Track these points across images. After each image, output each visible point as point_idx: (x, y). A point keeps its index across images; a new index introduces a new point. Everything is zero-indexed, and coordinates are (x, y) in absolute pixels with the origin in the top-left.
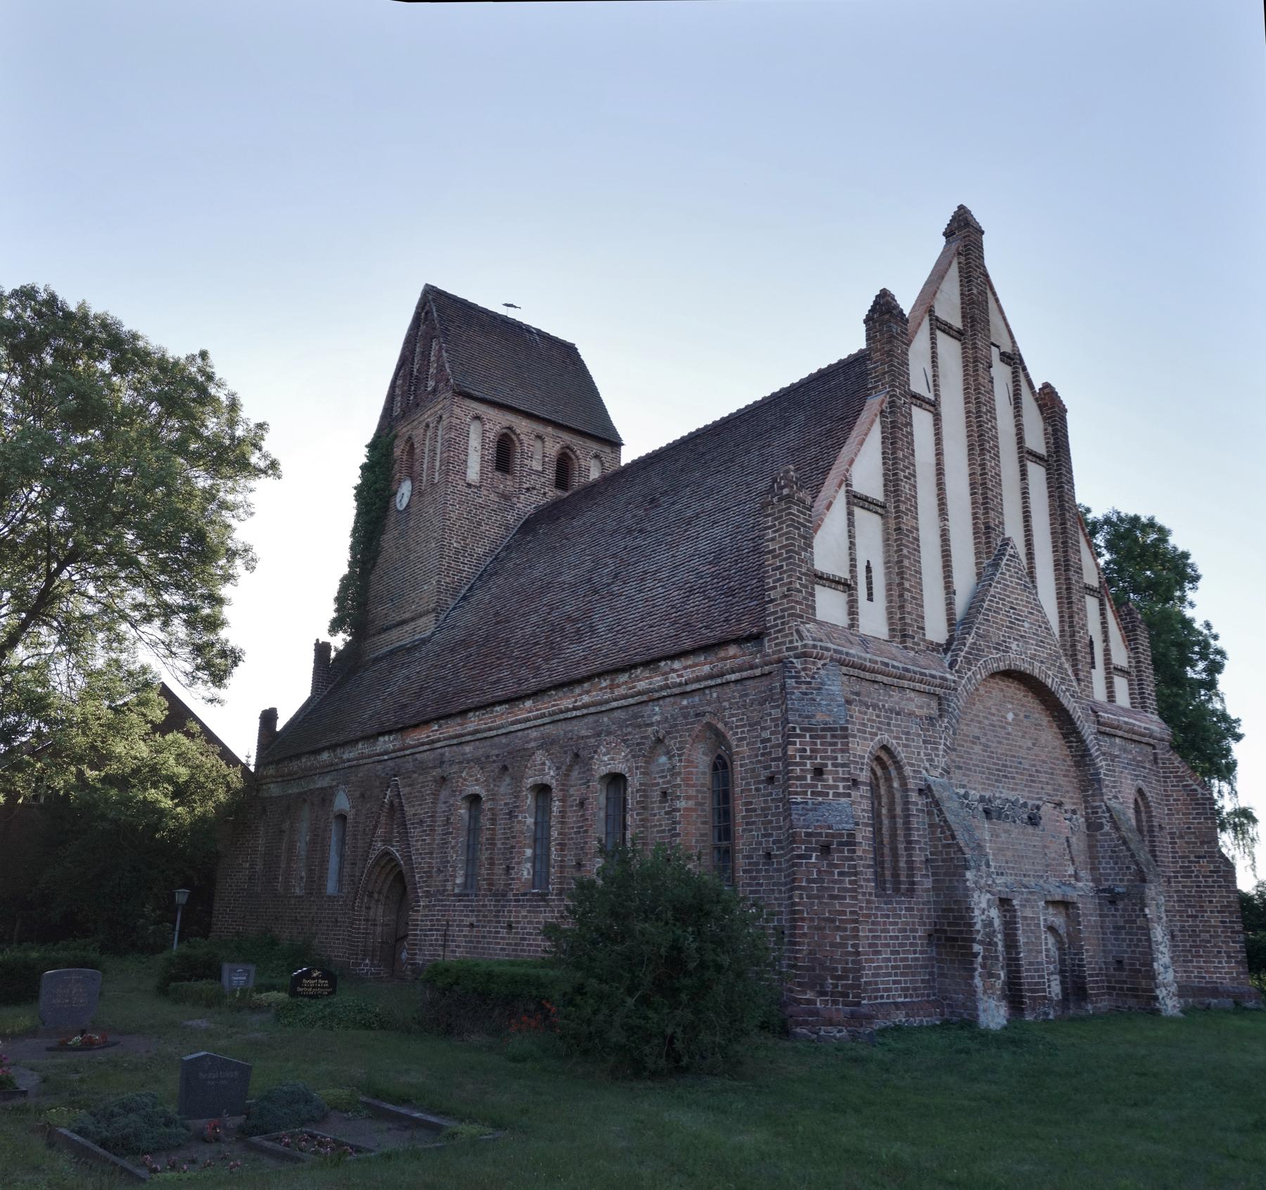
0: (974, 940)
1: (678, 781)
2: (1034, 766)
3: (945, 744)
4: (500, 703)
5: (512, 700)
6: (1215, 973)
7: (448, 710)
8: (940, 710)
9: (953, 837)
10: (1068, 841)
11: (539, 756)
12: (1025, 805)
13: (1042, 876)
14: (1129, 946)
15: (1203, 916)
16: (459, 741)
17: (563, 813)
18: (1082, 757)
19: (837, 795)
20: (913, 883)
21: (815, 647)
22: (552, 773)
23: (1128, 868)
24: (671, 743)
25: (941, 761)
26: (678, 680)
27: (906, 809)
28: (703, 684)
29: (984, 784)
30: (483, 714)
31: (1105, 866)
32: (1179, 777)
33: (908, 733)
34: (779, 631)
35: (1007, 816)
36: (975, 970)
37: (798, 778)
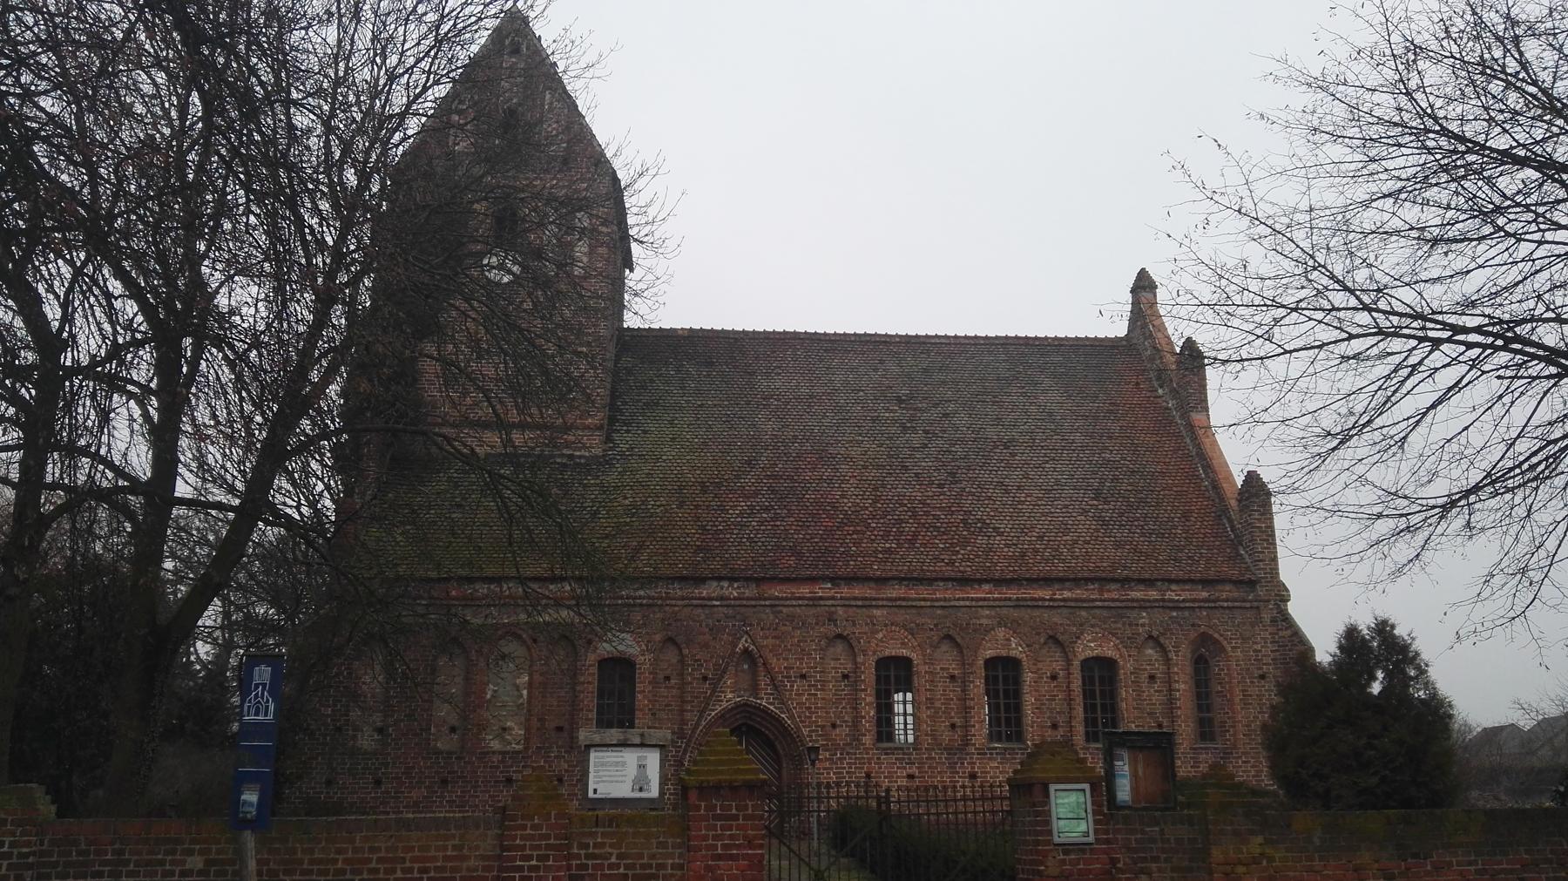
16: (868, 603)
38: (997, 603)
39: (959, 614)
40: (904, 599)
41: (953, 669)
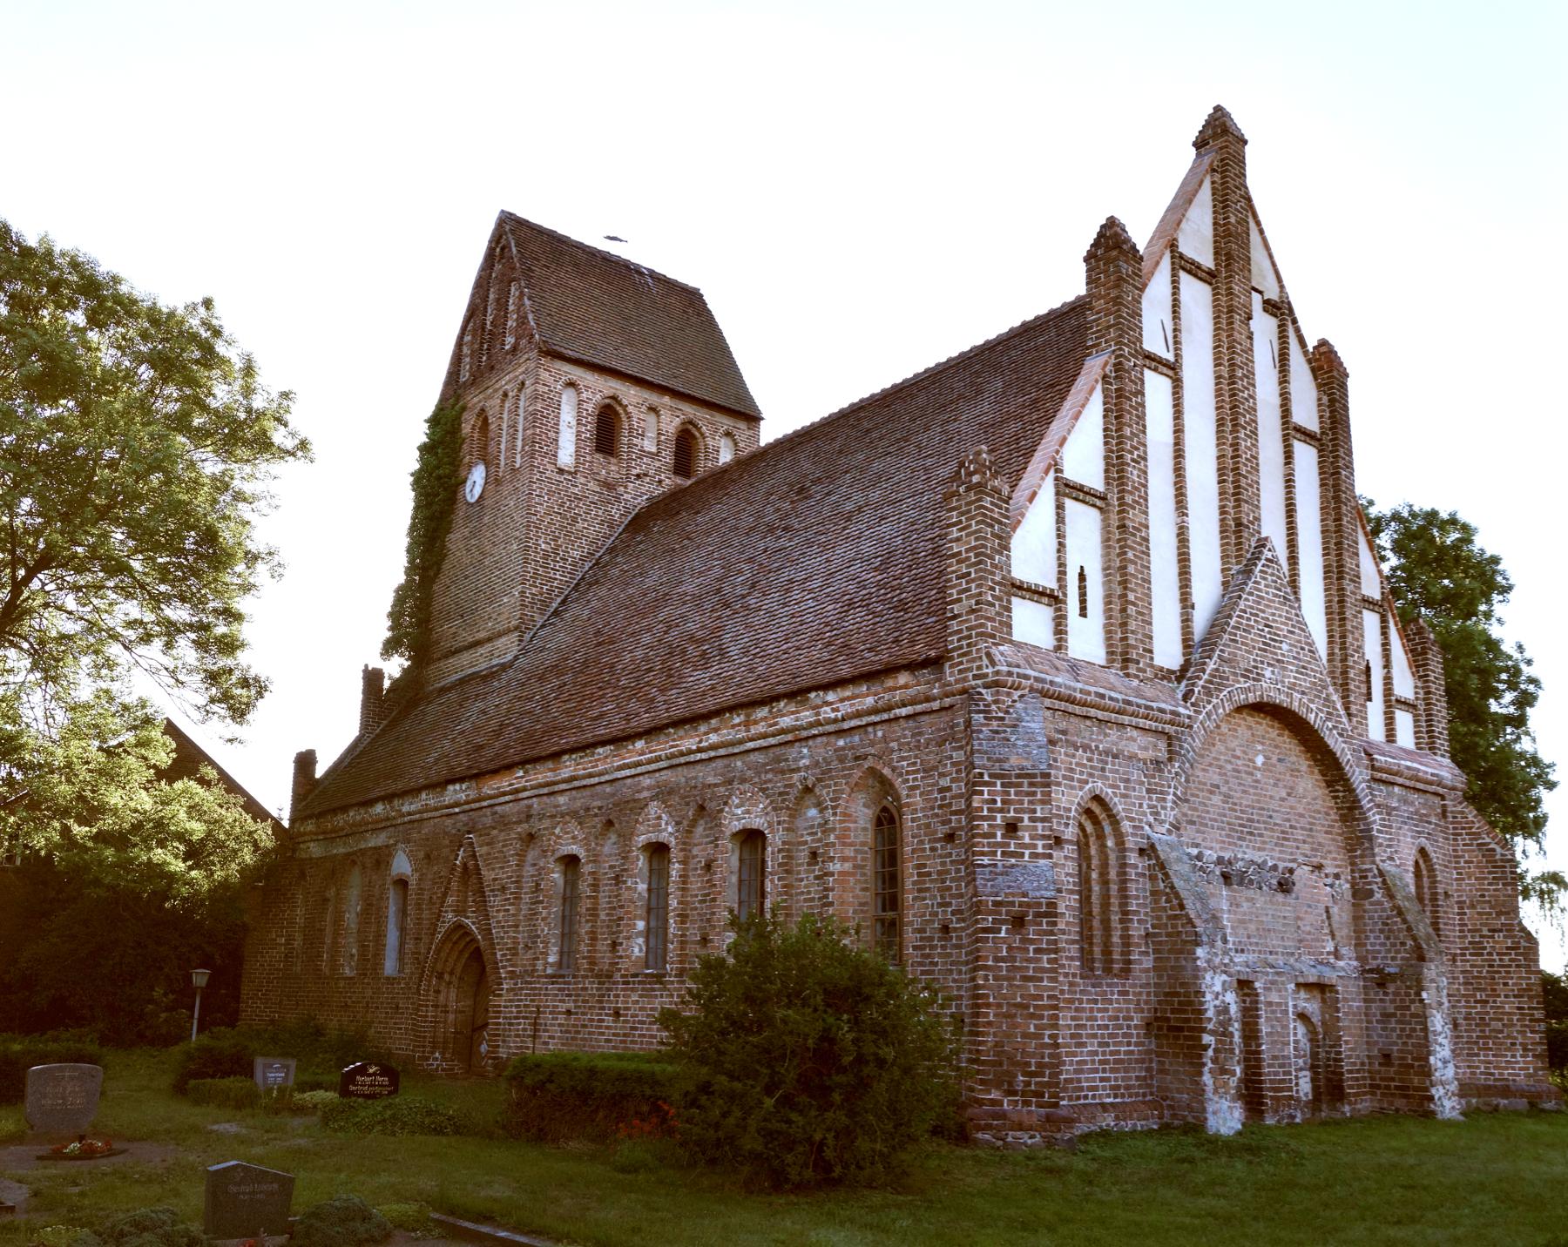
0: (1204, 1030)
1: (832, 838)
2: (1289, 820)
3: (1175, 794)
4: (603, 743)
5: (619, 740)
6: (1507, 1069)
7: (536, 753)
8: (1170, 752)
9: (1182, 907)
10: (1327, 912)
11: (654, 809)
12: (1275, 868)
13: (1293, 954)
14: (1399, 1037)
15: (1495, 1002)
17: (684, 878)
18: (1349, 810)
19: (1035, 856)
20: (1129, 962)
21: (1010, 674)
22: (670, 829)
23: (1403, 944)
24: (824, 793)
25: (1169, 815)
26: (833, 715)
27: (1122, 873)
28: (865, 720)
29: (1224, 842)
31: (1374, 942)
32: (1474, 833)
33: (1127, 781)
34: (964, 655)
35: (1251, 882)
36: (1204, 1065)
37: (985, 836)
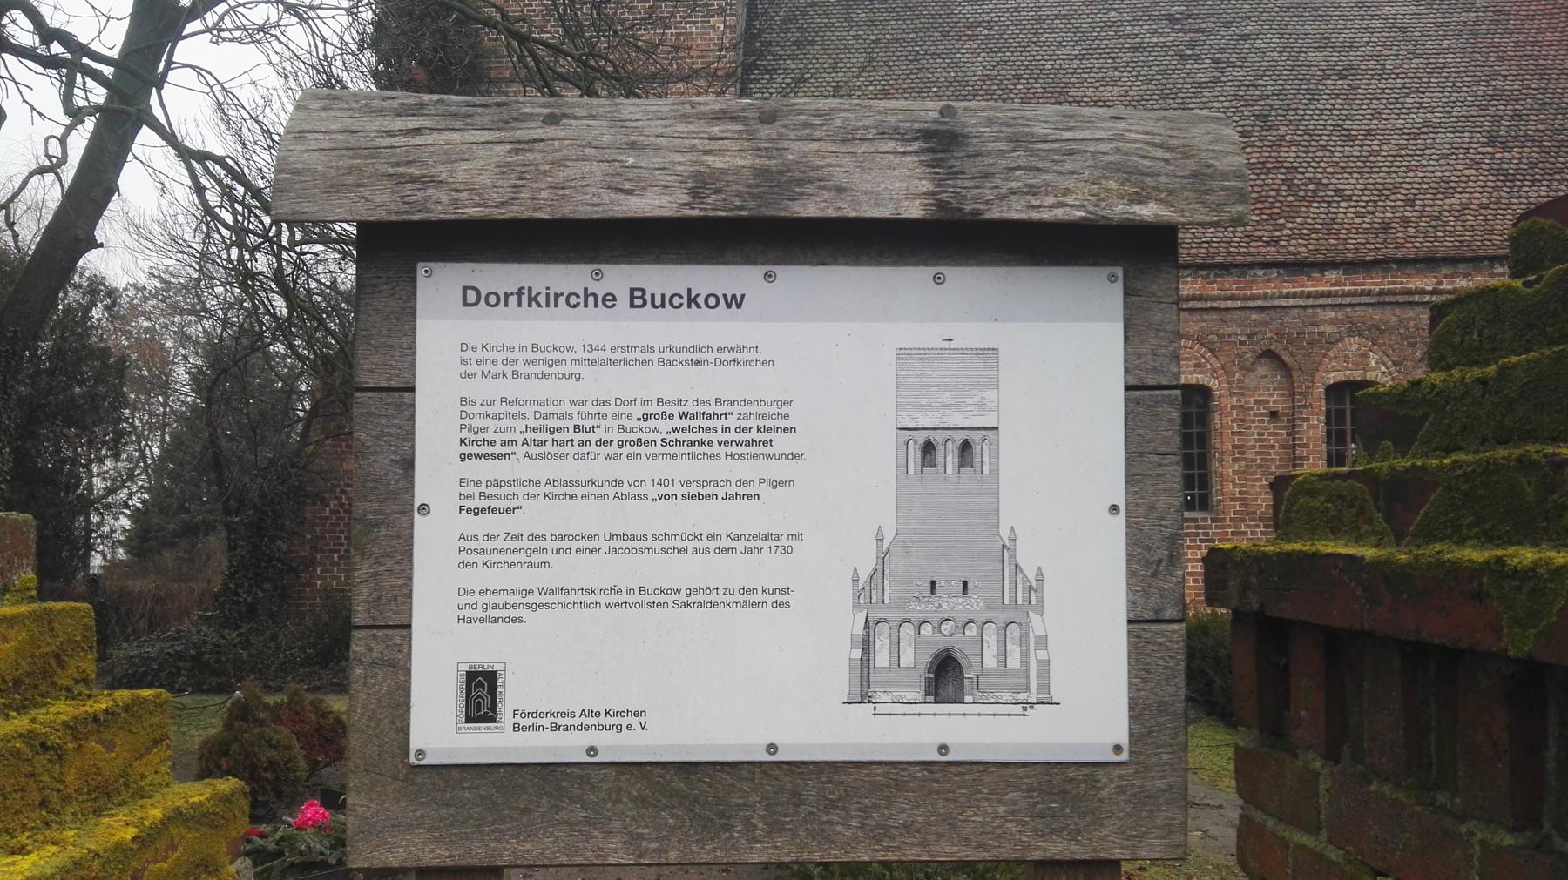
30: (1216, 275)
38: (1348, 300)
39: (1286, 319)
40: (1200, 298)
41: (1275, 402)
